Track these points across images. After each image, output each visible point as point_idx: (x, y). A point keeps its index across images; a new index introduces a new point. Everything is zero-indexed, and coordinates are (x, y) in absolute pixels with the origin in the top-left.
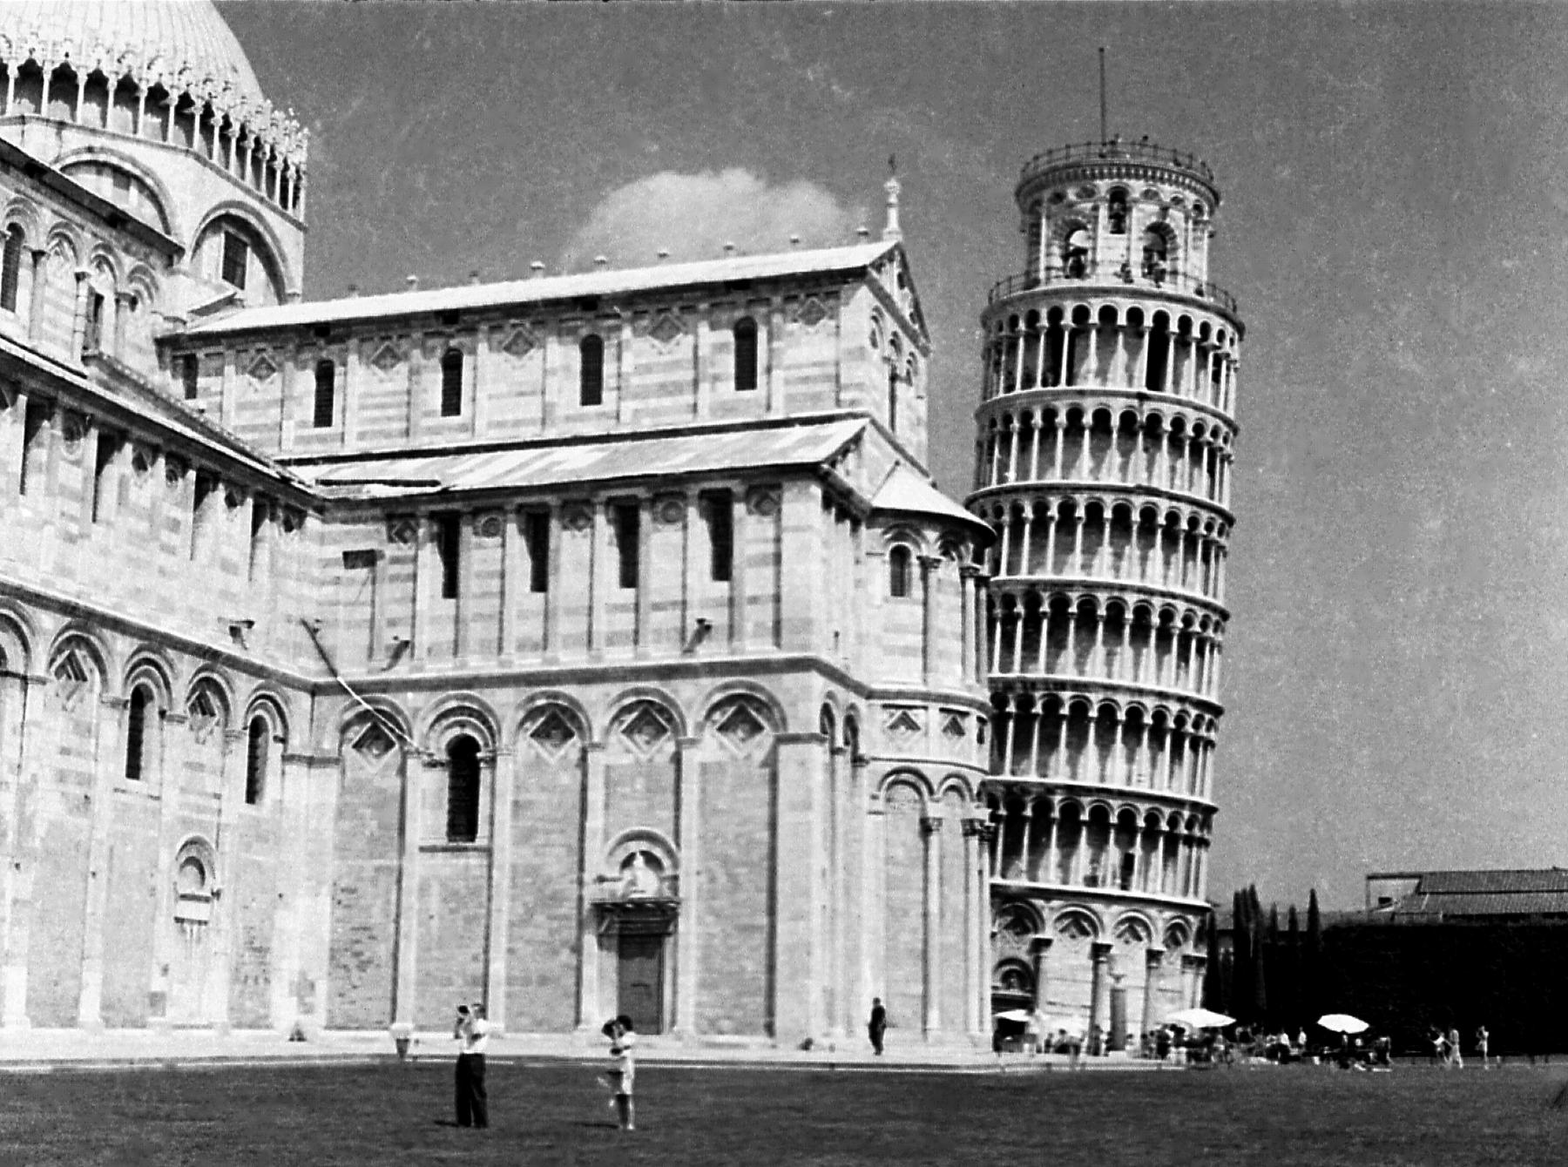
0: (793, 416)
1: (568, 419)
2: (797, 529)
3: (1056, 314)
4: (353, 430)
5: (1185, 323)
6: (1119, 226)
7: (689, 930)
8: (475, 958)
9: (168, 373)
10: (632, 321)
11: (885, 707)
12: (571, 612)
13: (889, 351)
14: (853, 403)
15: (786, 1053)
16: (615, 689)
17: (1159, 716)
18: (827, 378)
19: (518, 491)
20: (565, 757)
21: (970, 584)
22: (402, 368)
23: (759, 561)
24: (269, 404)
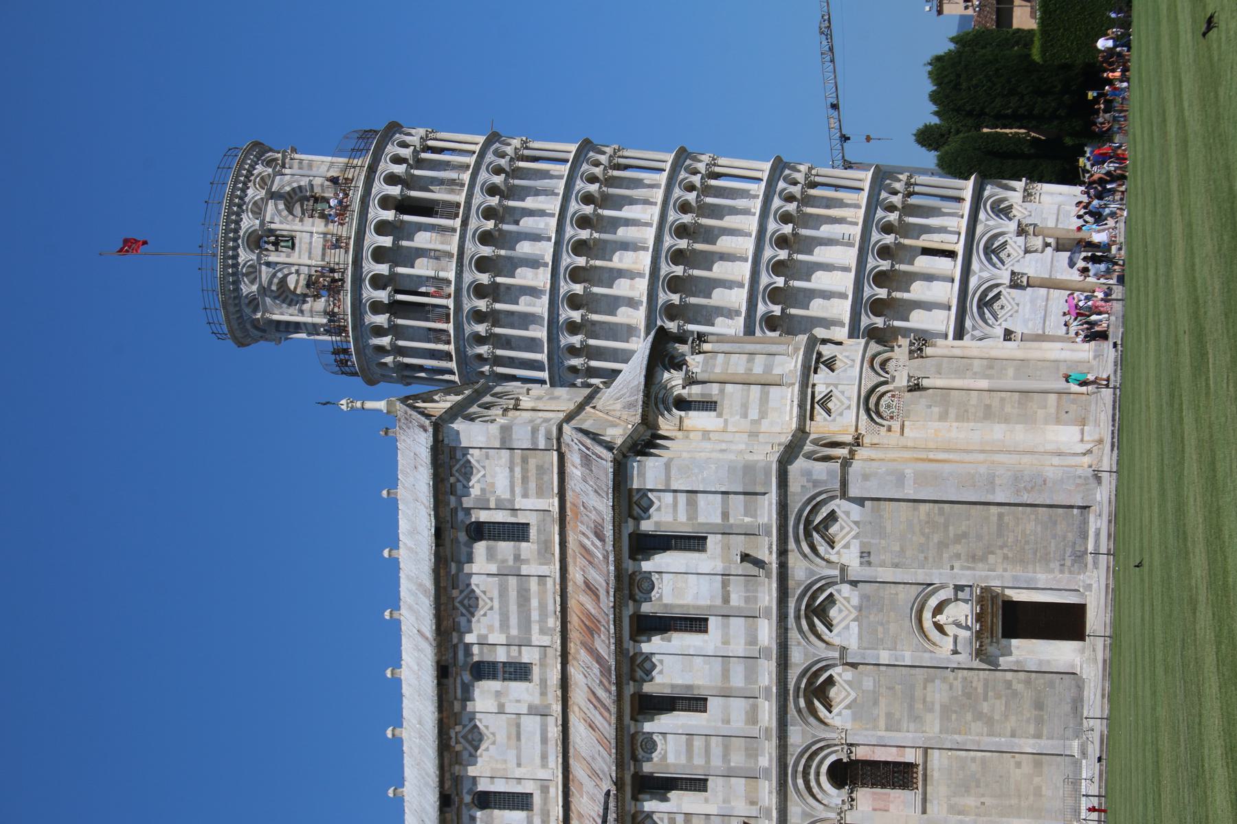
0: (556, 490)
1: (543, 693)
3: (377, 307)
5: (392, 179)
8: (1018, 765)
11: (812, 419)
12: (726, 674)
13: (496, 411)
14: (548, 439)
15: (1103, 495)
16: (794, 635)
18: (525, 461)
19: (620, 718)
20: (847, 682)
21: (706, 347)
23: (692, 505)
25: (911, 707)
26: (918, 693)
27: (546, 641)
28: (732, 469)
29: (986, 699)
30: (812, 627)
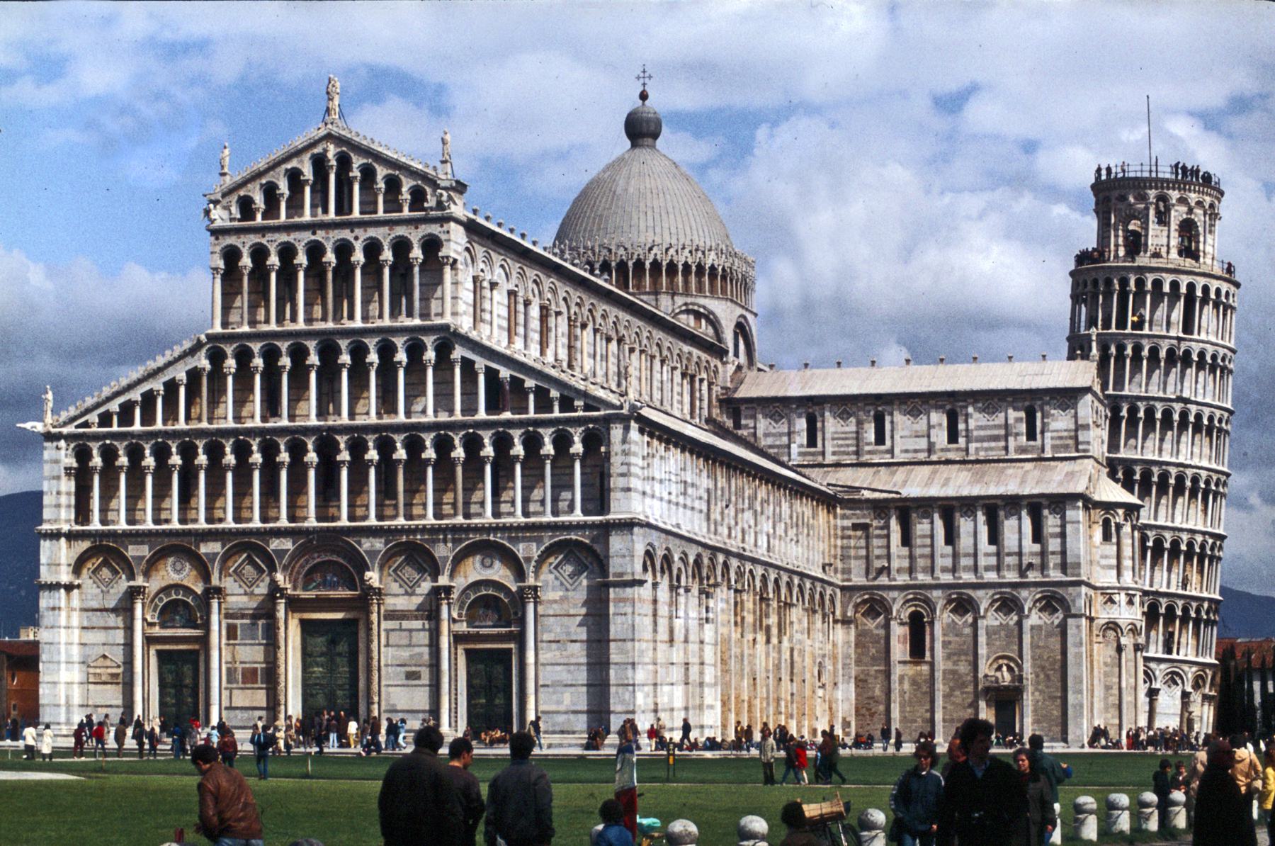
0: (1056, 455)
1: (942, 450)
2: (1073, 522)
4: (829, 449)
5: (1206, 289)
6: (1163, 219)
7: (1029, 699)
8: (927, 711)
9: (725, 416)
10: (973, 404)
11: (1102, 594)
12: (967, 555)
14: (1085, 451)
16: (991, 592)
17: (1190, 544)
18: (1071, 438)
20: (966, 621)
22: (853, 420)
24: (781, 435)
25: (955, 654)
26: (963, 658)
27: (972, 450)
28: (1078, 557)
29: (962, 693)
30: (995, 601)
